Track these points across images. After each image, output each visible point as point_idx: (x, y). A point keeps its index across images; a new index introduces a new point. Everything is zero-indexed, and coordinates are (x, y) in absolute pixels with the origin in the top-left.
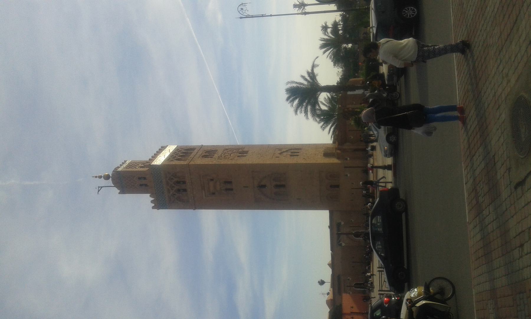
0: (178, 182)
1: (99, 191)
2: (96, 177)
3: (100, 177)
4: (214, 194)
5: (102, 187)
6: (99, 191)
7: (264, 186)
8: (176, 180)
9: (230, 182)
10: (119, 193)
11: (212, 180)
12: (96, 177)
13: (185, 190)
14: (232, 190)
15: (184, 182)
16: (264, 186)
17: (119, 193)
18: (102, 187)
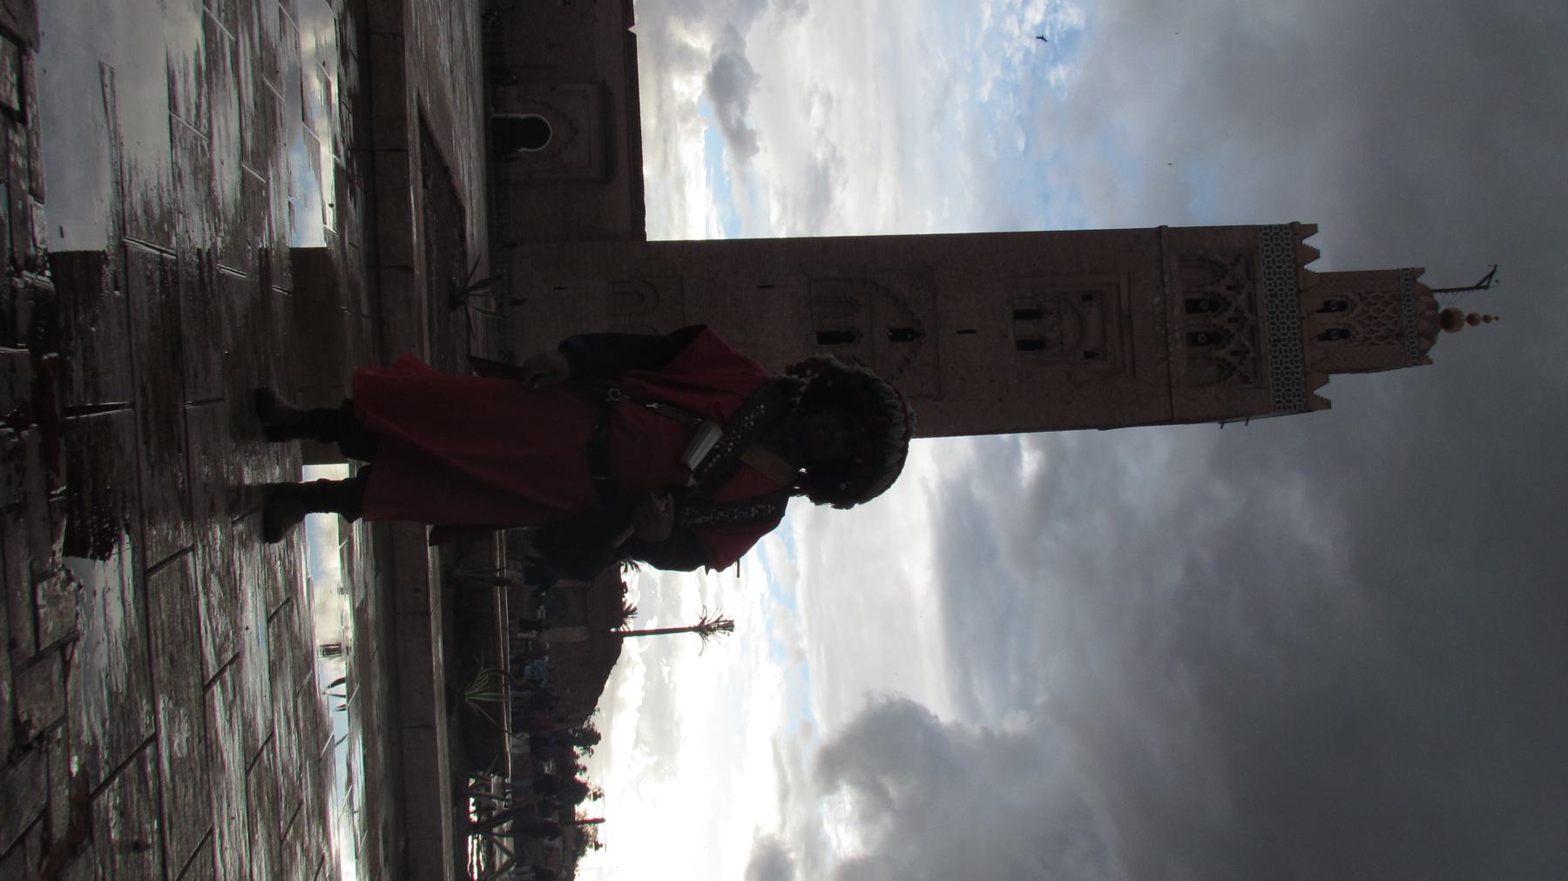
0: (1215, 339)
1: (1490, 276)
2: (1487, 319)
3: (1472, 320)
4: (1087, 297)
5: (1478, 287)
6: (1490, 276)
7: (898, 335)
8: (1222, 353)
9: (1024, 345)
10: (1421, 271)
11: (1090, 355)
12: (1487, 319)
13: (1192, 306)
14: (1020, 315)
15: (1192, 339)
16: (898, 335)
17: (1421, 271)
18: (1478, 287)
